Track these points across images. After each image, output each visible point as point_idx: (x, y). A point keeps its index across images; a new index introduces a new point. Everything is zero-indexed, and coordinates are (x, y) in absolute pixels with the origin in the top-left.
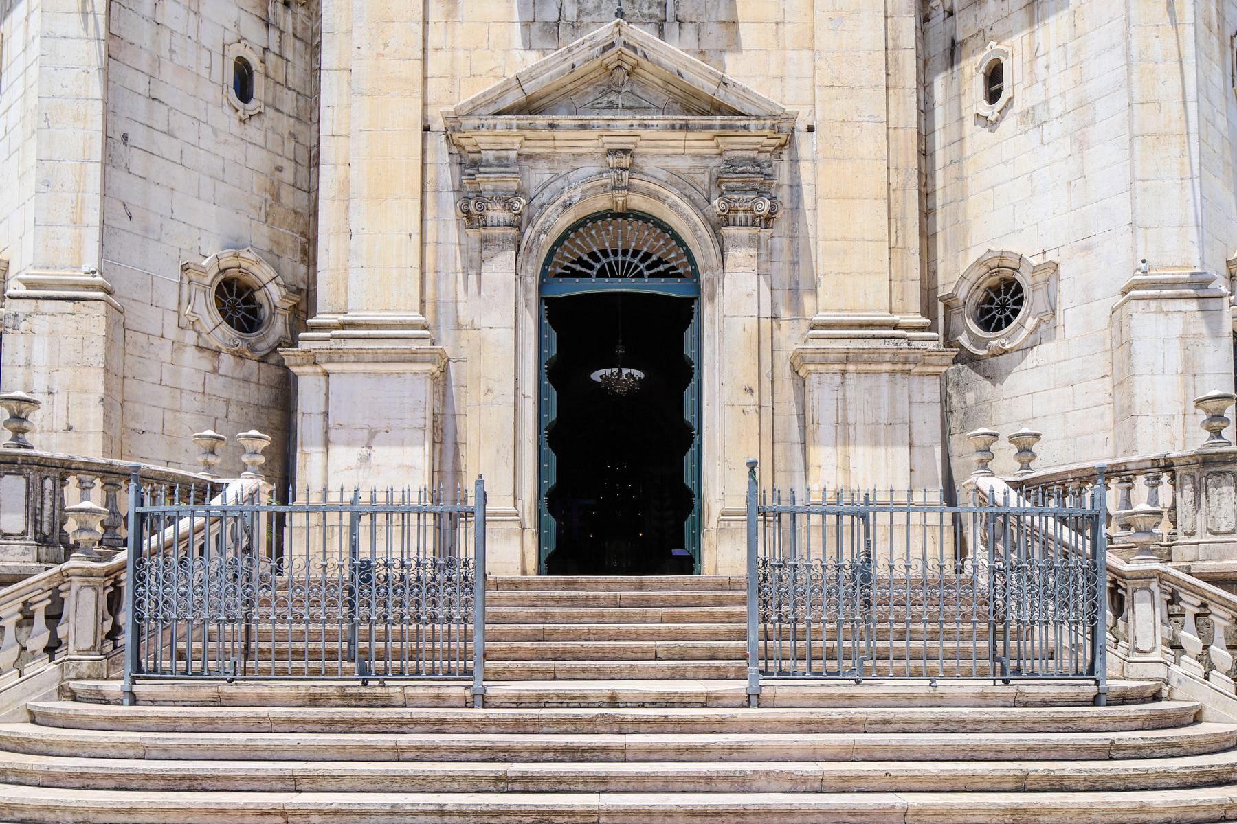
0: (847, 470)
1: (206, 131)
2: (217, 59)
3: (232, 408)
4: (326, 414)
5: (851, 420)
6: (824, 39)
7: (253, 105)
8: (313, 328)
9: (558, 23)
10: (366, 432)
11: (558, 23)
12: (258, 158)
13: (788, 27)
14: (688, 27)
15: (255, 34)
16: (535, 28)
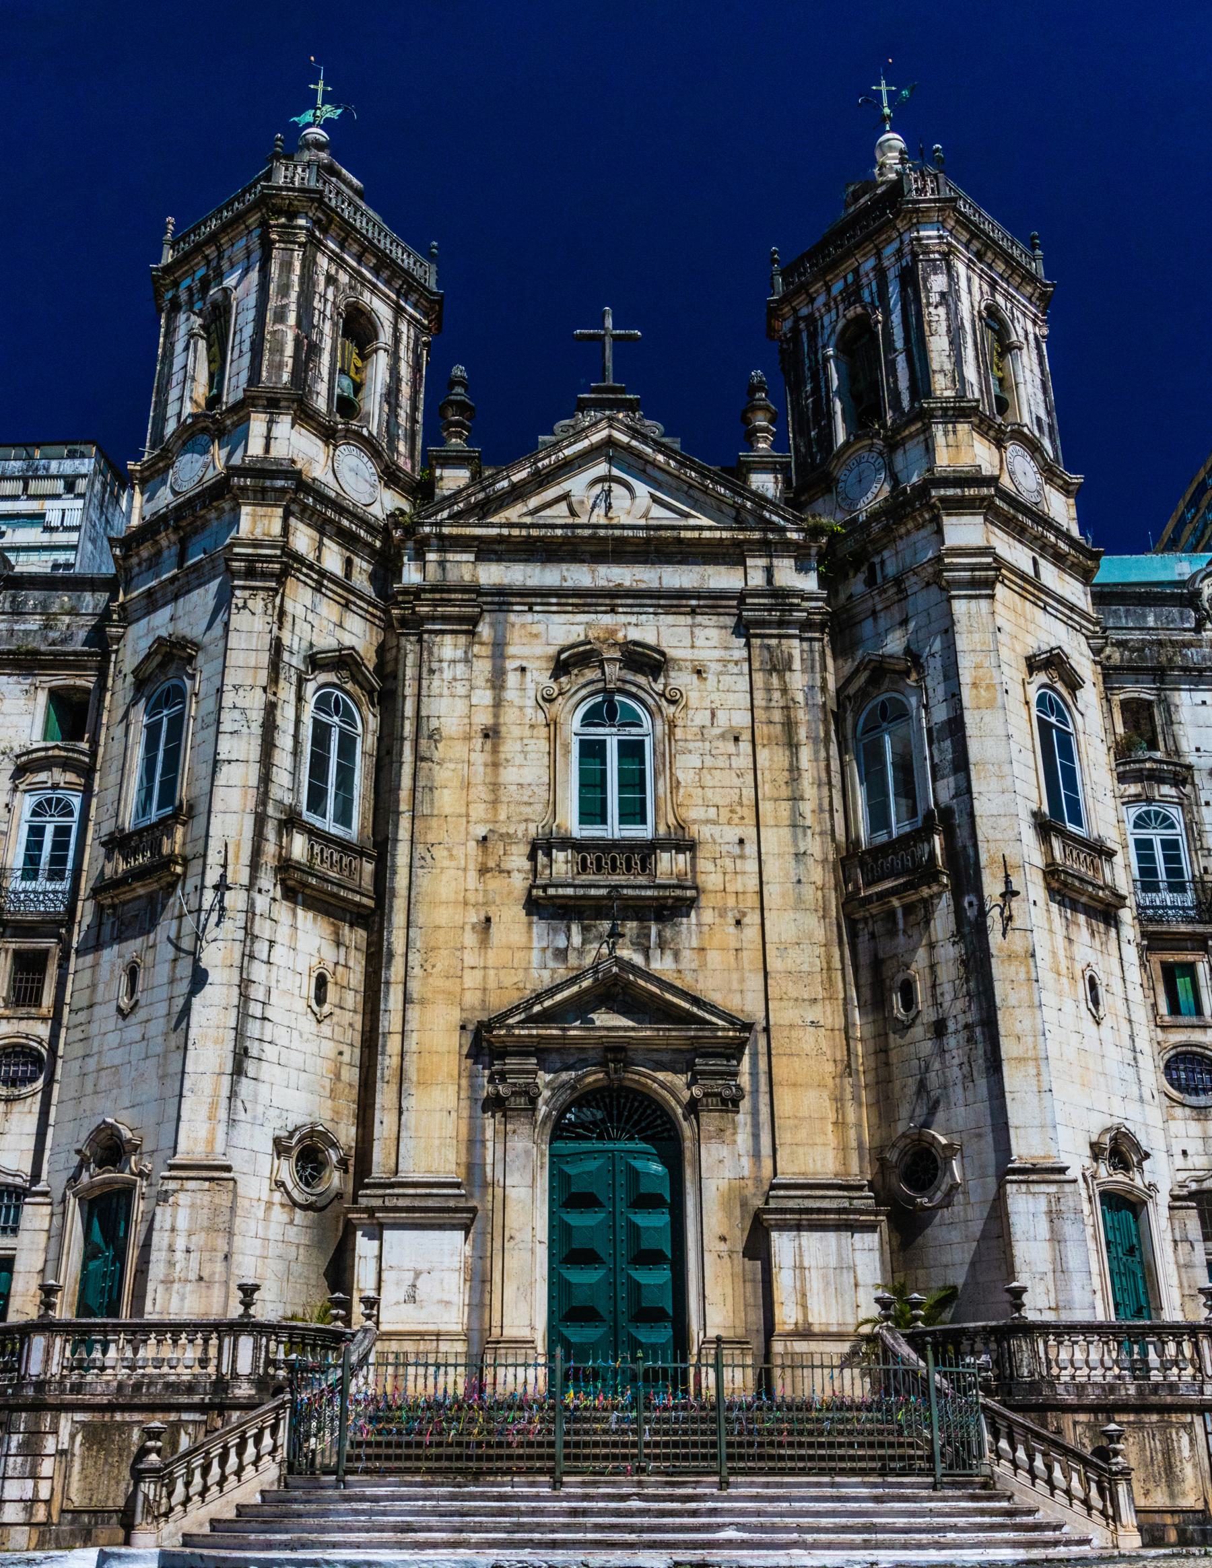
0: (804, 1307)
1: (295, 1034)
2: (305, 978)
3: (301, 1251)
4: (380, 1258)
5: (806, 1264)
6: (774, 963)
7: (326, 1008)
8: (368, 1186)
9: (566, 949)
10: (412, 1274)
11: (566, 949)
12: (329, 1048)
13: (745, 954)
14: (668, 953)
15: (330, 954)
16: (549, 953)
